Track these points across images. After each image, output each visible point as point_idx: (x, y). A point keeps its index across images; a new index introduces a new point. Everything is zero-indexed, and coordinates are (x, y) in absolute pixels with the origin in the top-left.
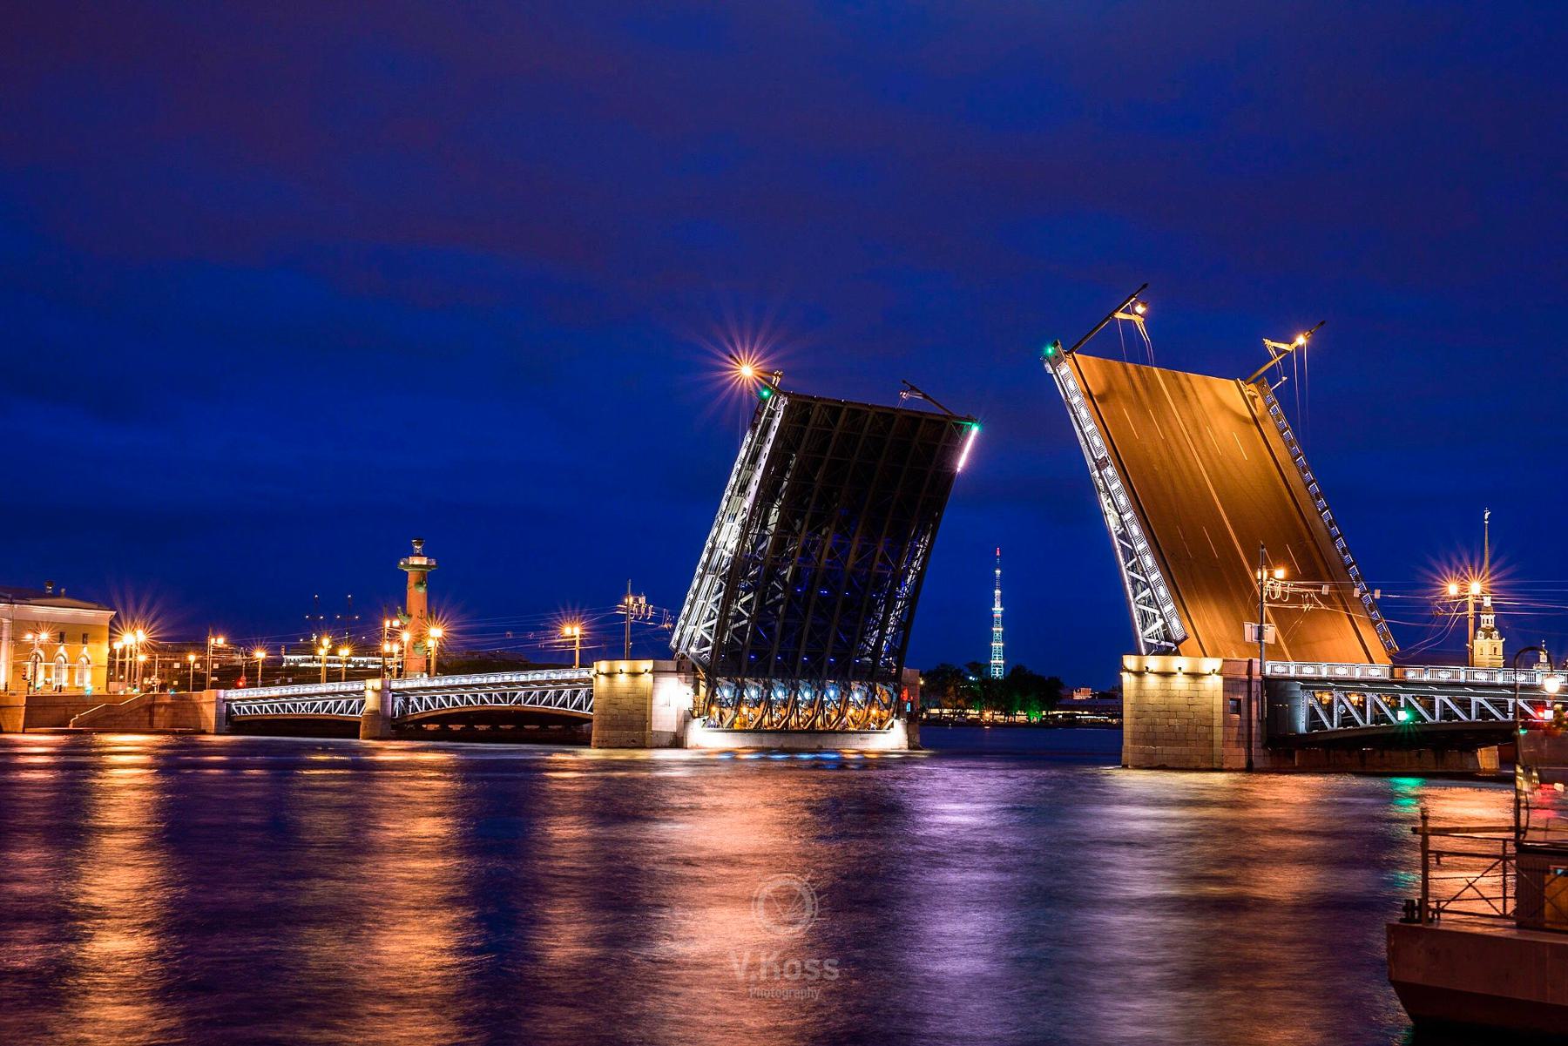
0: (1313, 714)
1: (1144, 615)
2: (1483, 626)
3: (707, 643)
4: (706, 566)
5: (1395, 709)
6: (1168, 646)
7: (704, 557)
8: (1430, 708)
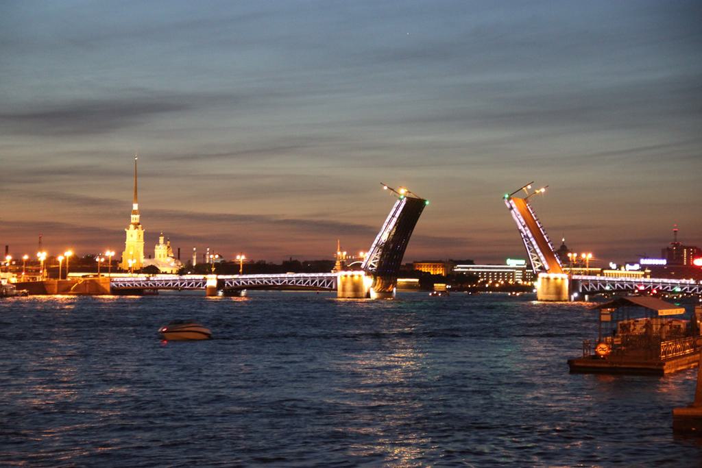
0: (583, 287)
1: (534, 264)
2: (132, 221)
3: (372, 267)
4: (377, 245)
5: (605, 285)
6: (542, 269)
7: (376, 242)
8: (614, 286)
